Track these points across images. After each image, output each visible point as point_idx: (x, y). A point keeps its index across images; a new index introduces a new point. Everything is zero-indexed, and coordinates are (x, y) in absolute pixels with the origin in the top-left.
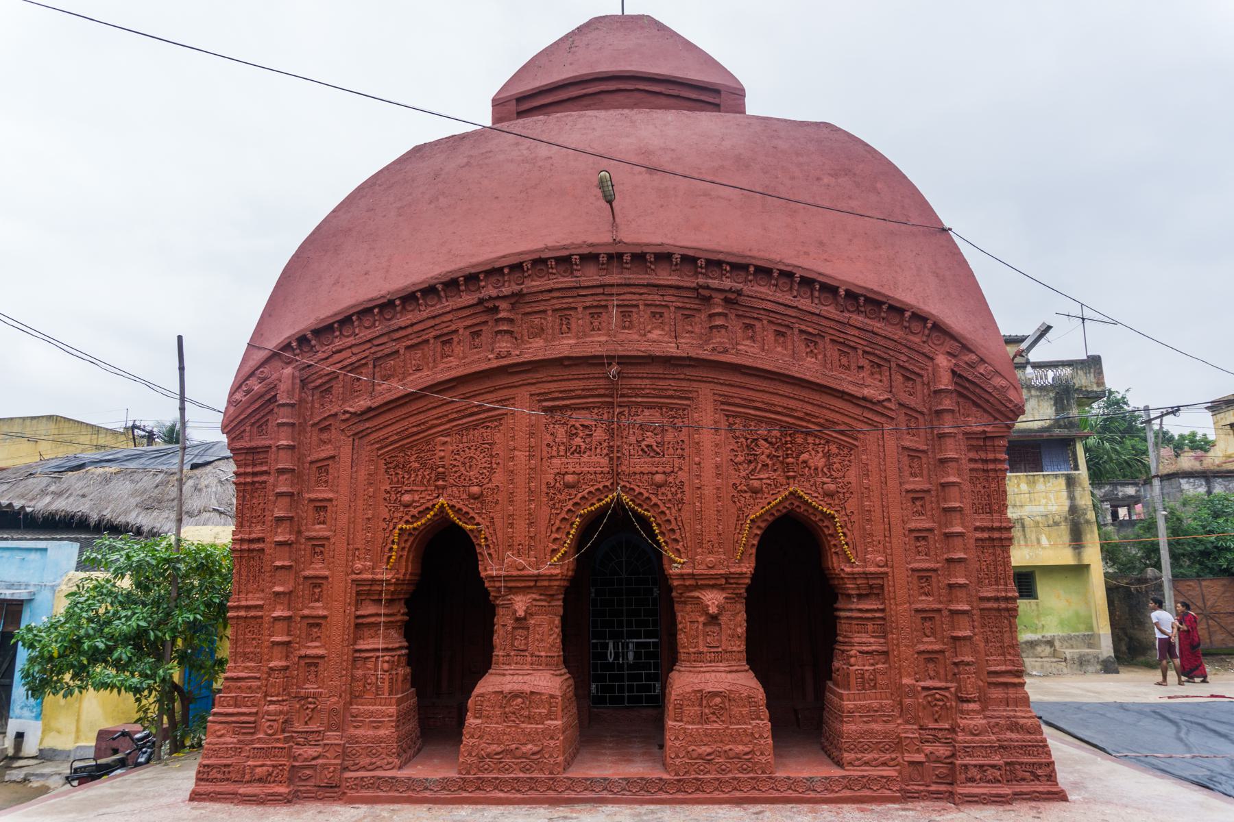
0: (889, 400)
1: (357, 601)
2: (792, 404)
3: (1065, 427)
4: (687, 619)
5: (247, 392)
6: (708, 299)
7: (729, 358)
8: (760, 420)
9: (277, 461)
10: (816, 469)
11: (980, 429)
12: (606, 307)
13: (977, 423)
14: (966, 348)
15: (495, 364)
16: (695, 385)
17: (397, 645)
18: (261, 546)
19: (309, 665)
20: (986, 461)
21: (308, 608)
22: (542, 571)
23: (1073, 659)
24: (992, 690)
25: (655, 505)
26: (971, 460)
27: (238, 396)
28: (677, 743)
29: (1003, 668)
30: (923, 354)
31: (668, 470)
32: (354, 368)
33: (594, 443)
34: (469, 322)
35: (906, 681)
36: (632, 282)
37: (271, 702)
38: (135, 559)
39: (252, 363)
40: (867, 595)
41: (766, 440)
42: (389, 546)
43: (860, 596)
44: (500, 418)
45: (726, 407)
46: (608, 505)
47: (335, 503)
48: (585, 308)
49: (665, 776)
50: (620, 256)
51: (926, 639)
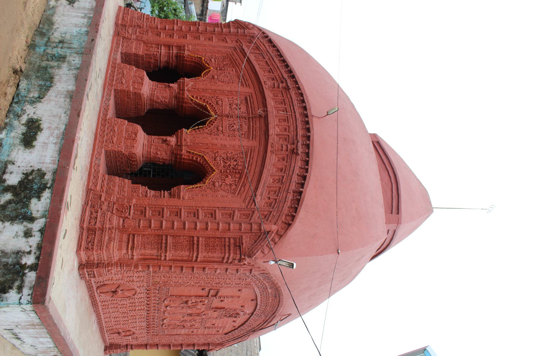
0: (255, 205)
2: (252, 172)
7: (269, 149)
13: (246, 241)
16: (258, 141)
20: (229, 246)
24: (127, 237)
26: (229, 238)
28: (119, 121)
29: (136, 242)
31: (224, 131)
32: (257, 48)
34: (277, 77)
35: (134, 201)
43: (170, 194)
45: (250, 151)
49: (108, 117)
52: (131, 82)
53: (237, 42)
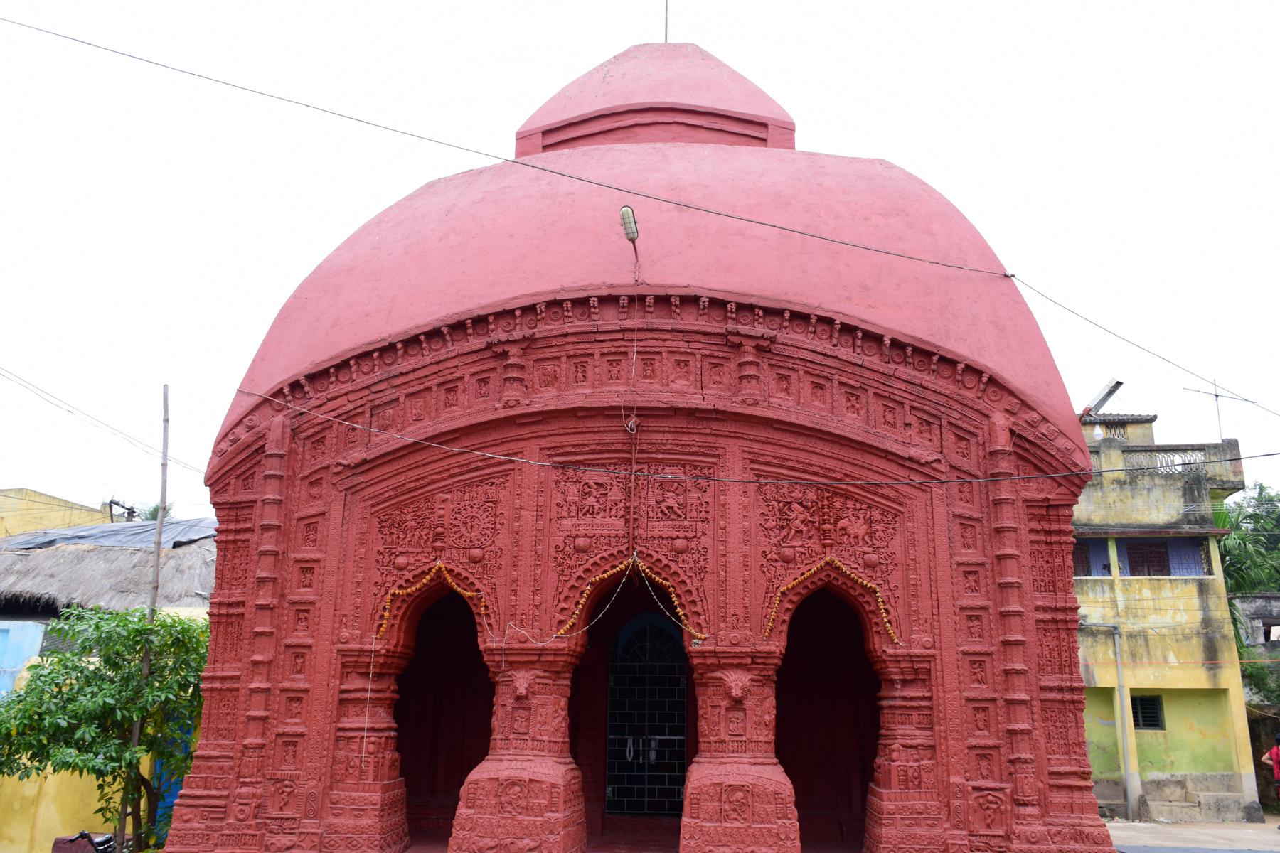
0: (939, 461)
1: (342, 674)
3: (1196, 522)
4: (710, 706)
5: (234, 442)
6: (737, 347)
8: (794, 482)
9: (262, 516)
10: (856, 537)
11: (1042, 496)
12: (625, 353)
13: (1039, 489)
14: (1025, 405)
15: (502, 414)
16: (722, 440)
17: (385, 725)
18: (241, 610)
19: (287, 744)
20: (1049, 533)
21: (289, 680)
22: (547, 645)
23: (1208, 804)
25: (675, 573)
26: (1032, 531)
27: (224, 446)
28: (692, 843)
29: (1068, 769)
30: (978, 411)
31: (690, 534)
33: (609, 504)
34: (476, 369)
35: (955, 779)
36: (655, 327)
37: (244, 784)
38: (105, 628)
39: (241, 411)
40: (912, 681)
41: (800, 504)
42: (380, 613)
43: (905, 682)
44: (506, 473)
45: (756, 466)
46: (622, 572)
47: (322, 564)
48: (603, 355)
50: (642, 298)
51: (978, 733)
52: (526, 819)
53: (317, 483)
